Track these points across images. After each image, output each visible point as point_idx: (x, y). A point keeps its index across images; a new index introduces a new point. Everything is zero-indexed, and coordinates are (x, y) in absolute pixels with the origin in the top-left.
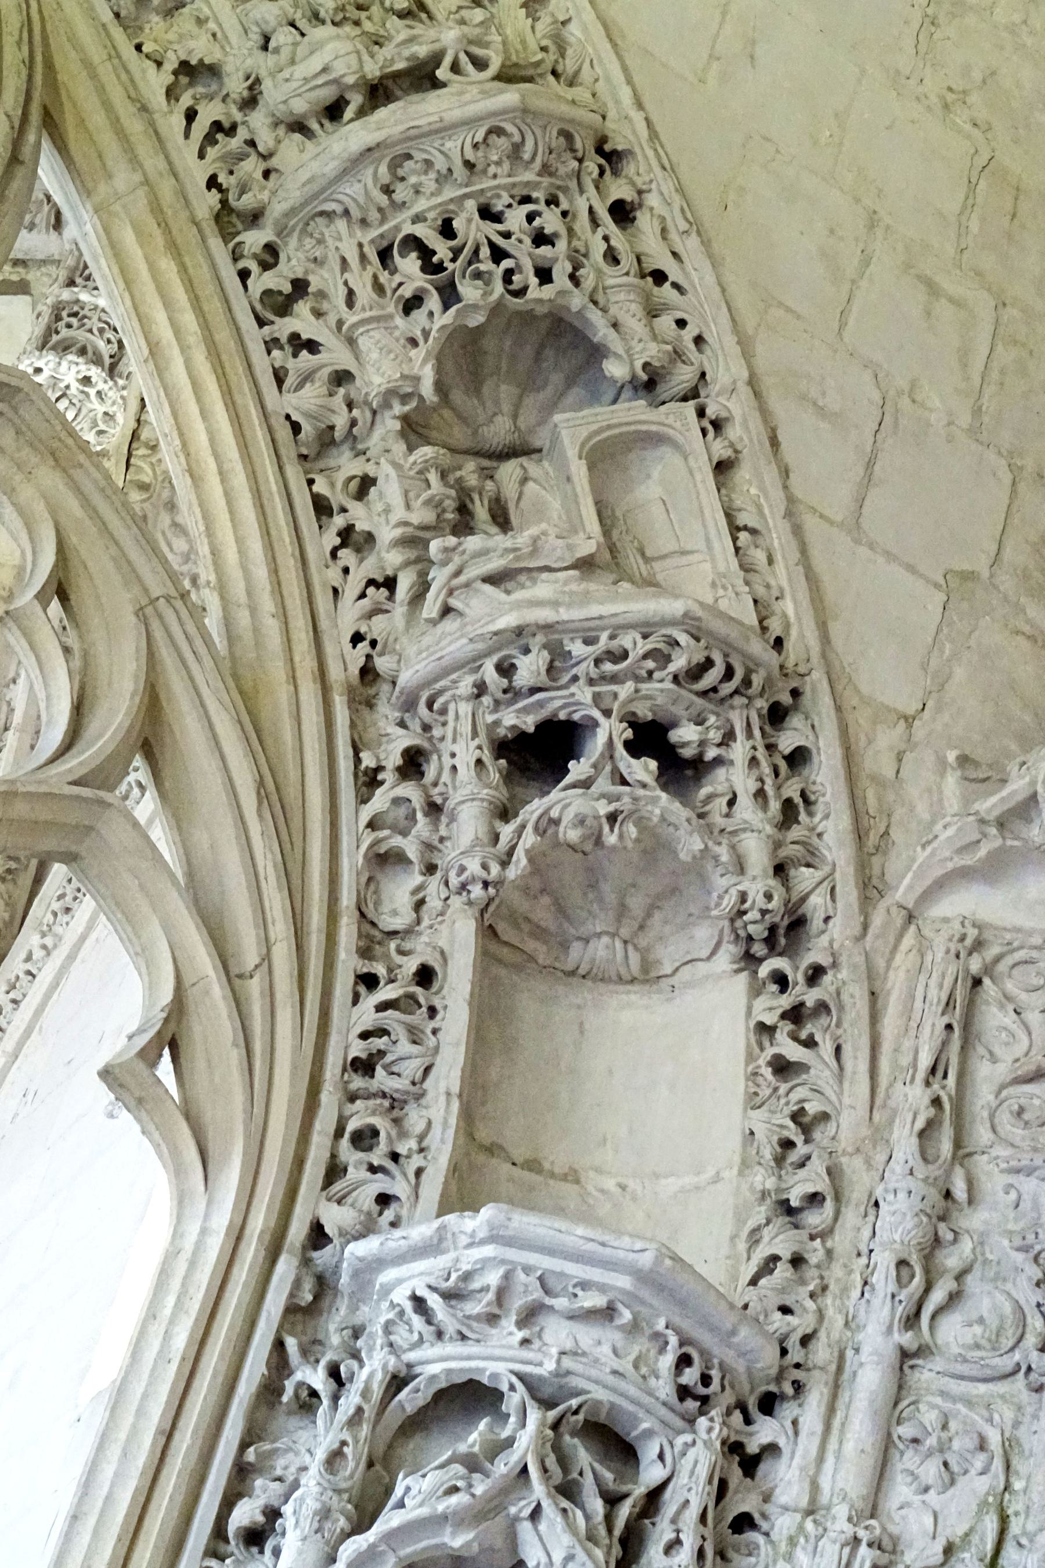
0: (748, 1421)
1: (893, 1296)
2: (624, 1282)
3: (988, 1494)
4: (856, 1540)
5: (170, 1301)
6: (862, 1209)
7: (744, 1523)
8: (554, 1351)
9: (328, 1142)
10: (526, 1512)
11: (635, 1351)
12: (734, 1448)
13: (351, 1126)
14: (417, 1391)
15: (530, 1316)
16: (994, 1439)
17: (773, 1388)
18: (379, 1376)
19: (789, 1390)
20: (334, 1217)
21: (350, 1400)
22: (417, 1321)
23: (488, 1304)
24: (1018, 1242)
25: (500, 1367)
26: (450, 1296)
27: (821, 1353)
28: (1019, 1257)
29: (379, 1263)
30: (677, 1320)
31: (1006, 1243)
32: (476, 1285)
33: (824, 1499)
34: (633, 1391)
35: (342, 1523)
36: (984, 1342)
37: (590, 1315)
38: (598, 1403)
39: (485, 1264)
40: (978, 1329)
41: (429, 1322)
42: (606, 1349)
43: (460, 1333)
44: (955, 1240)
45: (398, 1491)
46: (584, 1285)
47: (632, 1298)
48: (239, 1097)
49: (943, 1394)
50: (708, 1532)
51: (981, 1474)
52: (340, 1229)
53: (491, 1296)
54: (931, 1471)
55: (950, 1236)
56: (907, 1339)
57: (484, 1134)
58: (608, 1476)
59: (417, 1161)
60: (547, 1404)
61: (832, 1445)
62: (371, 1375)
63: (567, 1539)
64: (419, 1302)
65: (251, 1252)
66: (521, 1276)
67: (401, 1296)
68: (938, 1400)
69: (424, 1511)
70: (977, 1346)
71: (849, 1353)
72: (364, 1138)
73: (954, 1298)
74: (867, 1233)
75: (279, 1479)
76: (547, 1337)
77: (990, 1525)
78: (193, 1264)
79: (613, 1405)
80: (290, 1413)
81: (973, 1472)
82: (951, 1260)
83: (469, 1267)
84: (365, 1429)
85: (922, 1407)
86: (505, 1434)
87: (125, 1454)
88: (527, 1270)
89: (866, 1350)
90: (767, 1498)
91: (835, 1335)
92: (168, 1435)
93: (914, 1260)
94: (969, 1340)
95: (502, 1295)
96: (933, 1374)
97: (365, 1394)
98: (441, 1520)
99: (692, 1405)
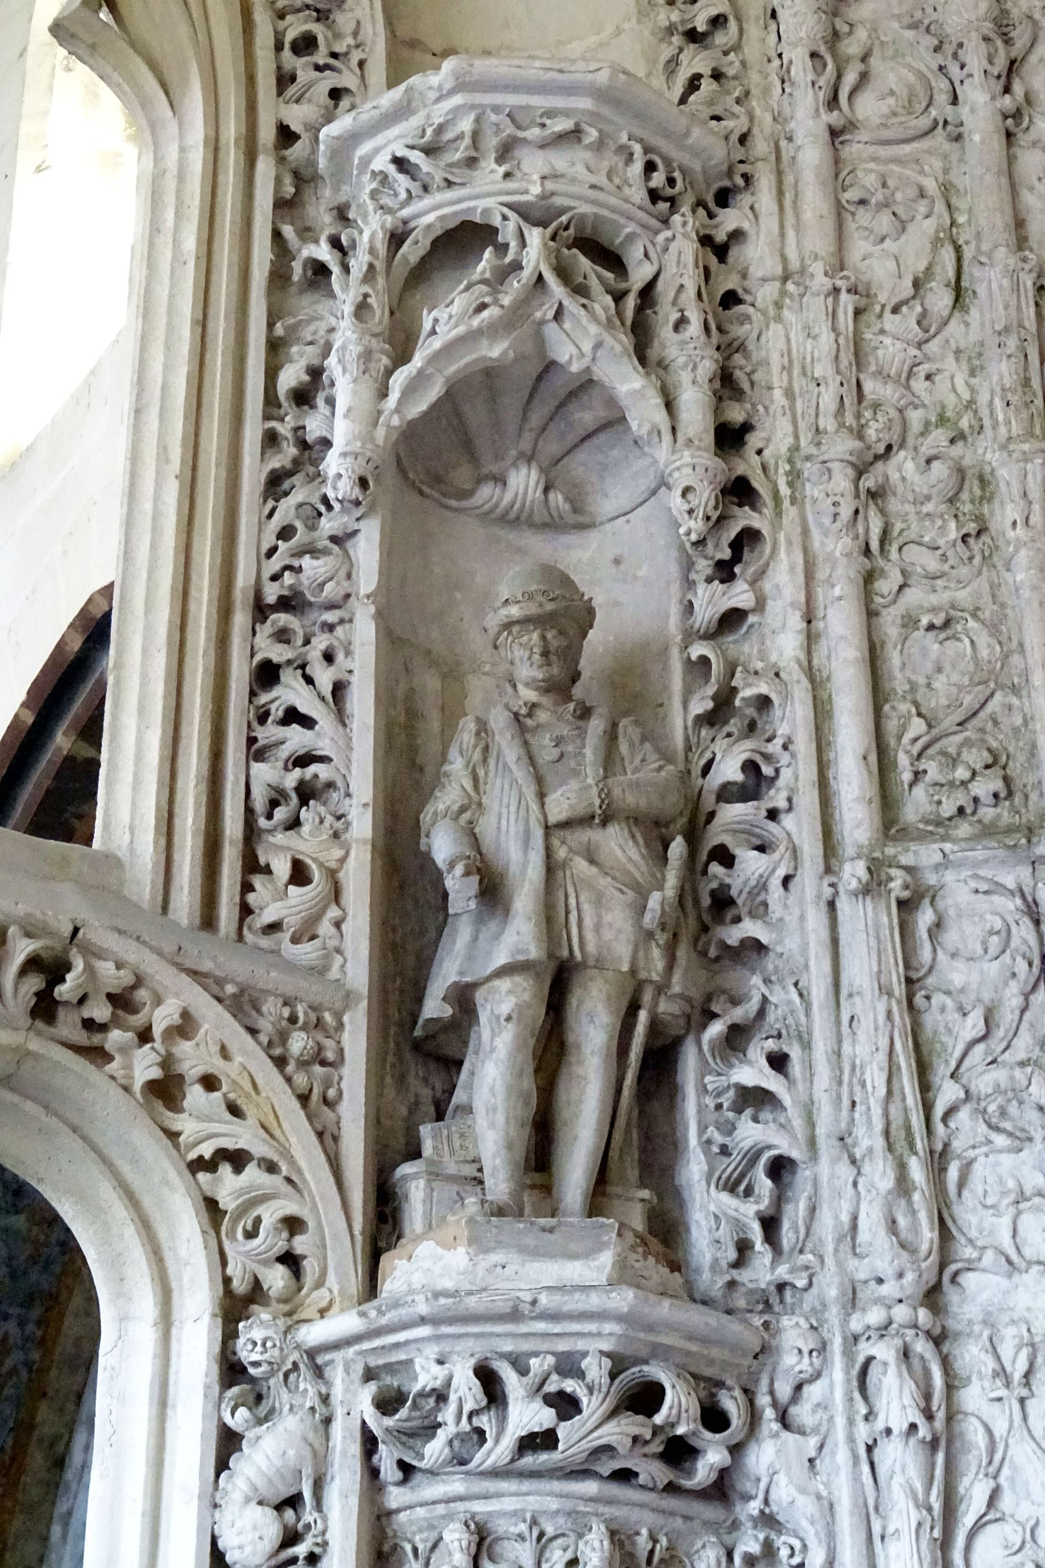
0: (711, 215)
1: (813, 84)
2: (585, 103)
3: (937, 231)
4: (836, 290)
5: (170, 216)
6: (762, 22)
7: (731, 299)
8: (536, 177)
9: (272, 54)
10: (550, 314)
11: (605, 165)
12: (706, 240)
13: (290, 36)
14: (417, 243)
15: (505, 152)
16: (931, 186)
17: (726, 183)
18: (380, 235)
19: (740, 182)
20: (296, 116)
21: (359, 263)
22: (402, 182)
23: (467, 148)
24: (907, 21)
25: (490, 202)
26: (430, 151)
27: (760, 146)
28: (910, 34)
29: (354, 138)
30: (638, 132)
31: (896, 25)
32: (449, 135)
33: (794, 264)
34: (612, 201)
35: (385, 361)
36: (900, 110)
37: (562, 138)
38: (583, 217)
39: (456, 112)
40: (891, 101)
41: (414, 179)
42: (580, 169)
43: (446, 180)
44: (850, 33)
45: (427, 325)
46: (550, 113)
47: (594, 117)
48: (183, 30)
49: (874, 159)
50: (706, 305)
51: (927, 217)
52: (305, 125)
53: (467, 141)
54: (884, 222)
55: (846, 28)
56: (834, 118)
57: (404, 31)
58: (609, 275)
59: (356, 56)
60: (543, 224)
61: (790, 219)
63: (593, 329)
64: (400, 163)
65: (232, 158)
66: (493, 117)
67: (382, 163)
68: (872, 165)
69: (461, 329)
70: (895, 114)
71: (783, 143)
72: (306, 45)
73: (864, 77)
74: (774, 37)
75: (311, 343)
76: (526, 167)
77: (947, 254)
78: (181, 177)
79: (595, 214)
80: (301, 292)
81: (919, 217)
82: (852, 47)
83: (441, 120)
84: (381, 281)
85: (860, 174)
86: (508, 259)
87: (168, 347)
88: (496, 109)
89: (800, 139)
90: (744, 276)
91: (767, 130)
92: (203, 324)
93: (823, 50)
94: (886, 111)
95: (476, 135)
96: (861, 146)
97: (372, 251)
99: (663, 206)
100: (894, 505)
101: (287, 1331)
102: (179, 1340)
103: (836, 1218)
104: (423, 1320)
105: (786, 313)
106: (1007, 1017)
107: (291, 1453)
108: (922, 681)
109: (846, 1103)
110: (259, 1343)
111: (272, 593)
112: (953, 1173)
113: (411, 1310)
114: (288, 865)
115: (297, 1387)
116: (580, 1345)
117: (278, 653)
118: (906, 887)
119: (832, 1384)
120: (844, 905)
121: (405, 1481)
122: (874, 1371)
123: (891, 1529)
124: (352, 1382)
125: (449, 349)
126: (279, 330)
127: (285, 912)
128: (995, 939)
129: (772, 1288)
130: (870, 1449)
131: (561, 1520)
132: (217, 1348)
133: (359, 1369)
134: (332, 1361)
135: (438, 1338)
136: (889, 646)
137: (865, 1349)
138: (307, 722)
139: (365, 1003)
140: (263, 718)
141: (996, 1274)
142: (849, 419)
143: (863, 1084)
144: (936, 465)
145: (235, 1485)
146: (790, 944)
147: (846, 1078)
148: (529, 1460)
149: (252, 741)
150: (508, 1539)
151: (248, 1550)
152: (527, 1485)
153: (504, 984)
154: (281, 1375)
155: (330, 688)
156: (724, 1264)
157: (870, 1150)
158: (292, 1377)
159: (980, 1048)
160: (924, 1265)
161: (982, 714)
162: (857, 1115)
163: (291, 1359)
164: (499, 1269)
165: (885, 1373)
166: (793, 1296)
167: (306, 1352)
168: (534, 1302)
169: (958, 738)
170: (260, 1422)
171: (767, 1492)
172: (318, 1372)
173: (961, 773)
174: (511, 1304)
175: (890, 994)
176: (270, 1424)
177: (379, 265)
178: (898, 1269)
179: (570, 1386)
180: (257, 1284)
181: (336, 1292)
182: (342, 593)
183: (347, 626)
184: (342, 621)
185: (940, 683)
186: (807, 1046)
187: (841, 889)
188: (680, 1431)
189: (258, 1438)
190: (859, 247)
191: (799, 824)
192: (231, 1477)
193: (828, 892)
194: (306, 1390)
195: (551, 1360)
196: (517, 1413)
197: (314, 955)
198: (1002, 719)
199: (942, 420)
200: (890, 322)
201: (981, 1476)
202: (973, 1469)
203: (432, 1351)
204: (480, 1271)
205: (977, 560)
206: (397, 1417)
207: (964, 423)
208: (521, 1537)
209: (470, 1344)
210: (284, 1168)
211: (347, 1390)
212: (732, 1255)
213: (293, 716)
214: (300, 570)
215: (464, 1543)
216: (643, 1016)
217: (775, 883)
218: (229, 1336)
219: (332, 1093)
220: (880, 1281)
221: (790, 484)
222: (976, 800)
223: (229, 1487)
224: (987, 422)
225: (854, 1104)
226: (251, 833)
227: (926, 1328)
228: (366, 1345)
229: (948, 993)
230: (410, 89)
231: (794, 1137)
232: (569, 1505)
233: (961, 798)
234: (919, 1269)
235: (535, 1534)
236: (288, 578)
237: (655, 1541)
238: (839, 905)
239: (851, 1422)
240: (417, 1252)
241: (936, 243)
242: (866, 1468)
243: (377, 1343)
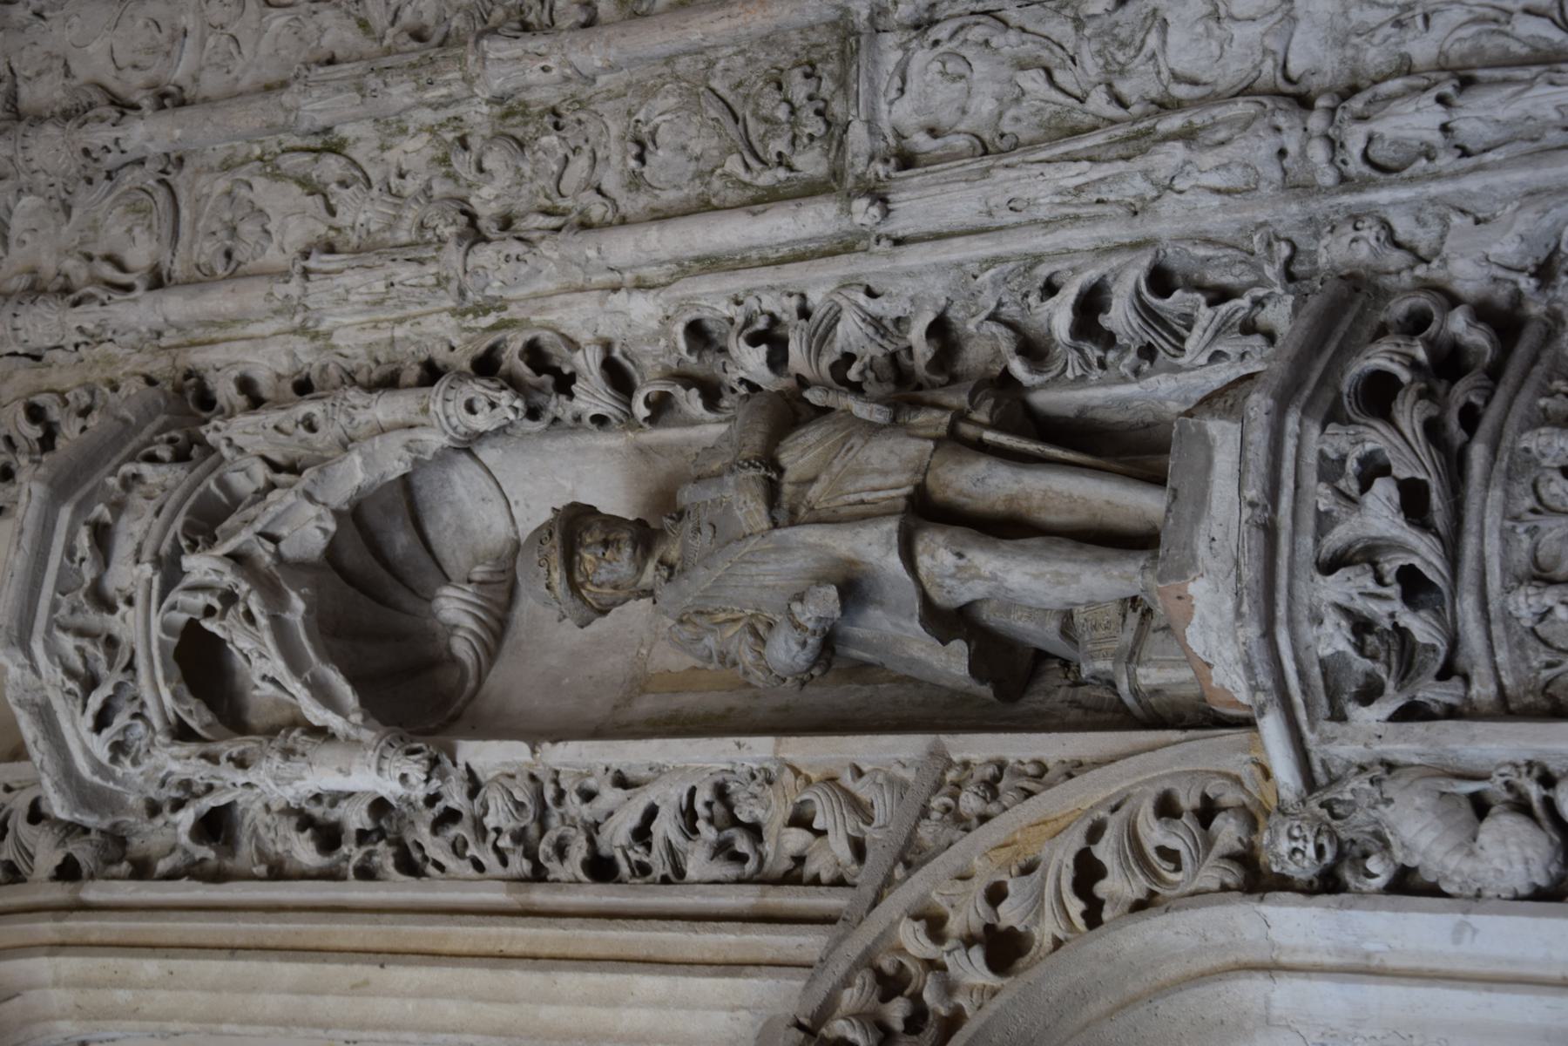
1: (103, 304)
2: (65, 514)
3: (266, 175)
5: (122, 996)
6: (44, 371)
8: (136, 571)
10: (270, 547)
14: (190, 712)
16: (222, 184)
19: (192, 381)
20: (47, 856)
21: (198, 771)
23: (95, 645)
24: (61, 216)
28: (76, 213)
31: (65, 229)
32: (78, 664)
34: (176, 495)
36: (146, 222)
39: (52, 651)
40: (137, 231)
43: (125, 670)
44: (67, 276)
46: (70, 552)
47: (83, 507)
51: (250, 186)
52: (57, 846)
53: (85, 643)
62: (176, 758)
66: (64, 611)
68: (196, 247)
70: (150, 227)
76: (125, 583)
79: (188, 513)
81: (251, 196)
83: (59, 670)
88: (55, 606)
89: (157, 320)
94: (145, 237)
95: (81, 632)
96: (176, 261)
98: (280, 630)
100: (520, 206)
101: (1282, 810)
102: (1294, 950)
103: (1216, 211)
104: (1269, 634)
105: (323, 327)
106: (1030, 48)
107: (1418, 801)
108: (692, 166)
109: (1098, 209)
110: (1294, 844)
111: (519, 865)
112: (1181, 91)
113: (1254, 649)
114: (793, 830)
115: (1350, 802)
116: (1311, 459)
117: (578, 851)
118: (886, 161)
119: (1394, 204)
120: (900, 225)
121: (1467, 679)
122: (1377, 153)
123: (1554, 116)
124: (1344, 735)
125: (296, 664)
126: (261, 869)
127: (841, 832)
128: (950, 67)
129: (1292, 286)
130: (1465, 153)
131: (1517, 489)
132: (1300, 897)
133: (1329, 727)
134: (1323, 763)
135: (1292, 622)
136: (656, 204)
137: (1356, 167)
138: (651, 813)
139: (945, 738)
140: (643, 869)
141: (1291, 35)
142: (429, 253)
143: (1079, 189)
144: (487, 164)
145: (1454, 872)
146: (937, 290)
147: (1071, 211)
148: (1439, 518)
149: (665, 880)
150: (1535, 548)
151: (1530, 852)
152: (1471, 524)
153: (924, 562)
154: (1334, 823)
155: (620, 791)
156: (1269, 351)
157: (1146, 174)
158: (1339, 810)
159: (1059, 76)
160: (1270, 105)
161: (730, 99)
162: (1112, 197)
163: (1317, 809)
164: (1215, 545)
165: (1381, 137)
166: (1302, 263)
167: (1310, 793)
168: (1252, 505)
169: (751, 123)
170: (1386, 846)
171: (1509, 268)
172: (1334, 781)
173: (782, 113)
174: (1254, 530)
175: (987, 170)
176: (1387, 831)
177: (203, 748)
178: (1270, 131)
179: (1352, 465)
180: (1232, 857)
181: (1246, 757)
182: (527, 782)
183: (561, 776)
184: (556, 782)
185: (696, 147)
186: (1038, 259)
187: (882, 230)
188: (1421, 354)
189: (1403, 846)
190: (273, 257)
191: (817, 283)
192: (1446, 878)
193: (885, 243)
194: (1353, 791)
195: (1323, 488)
196: (1377, 523)
197: (887, 797)
198: (737, 76)
199: (445, 161)
200: (343, 219)
201: (1508, 28)
202: (1502, 40)
203: (1308, 632)
204: (1213, 564)
205: (583, 116)
206: (1384, 676)
207: (450, 136)
208: (1533, 531)
209: (1302, 587)
210: (1102, 813)
211: (1353, 740)
212: (1257, 341)
213: (642, 834)
214: (498, 831)
215: (1531, 591)
216: (989, 436)
217: (874, 307)
218: (1283, 884)
219: (1031, 769)
220: (1282, 153)
221: (486, 312)
222: (811, 98)
223: (1457, 879)
224: (451, 112)
225: (1099, 201)
226: (761, 879)
227: (1336, 97)
228: (1302, 715)
229: (1000, 115)
230: (20, 703)
231: (1127, 264)
232: (1498, 477)
233: (807, 114)
234: (1273, 112)
235: (1531, 516)
236: (505, 842)
237: (1558, 391)
238: (900, 234)
239: (1437, 176)
240: (1200, 654)
241: (277, 175)
242: (1489, 157)
243: (1298, 699)
